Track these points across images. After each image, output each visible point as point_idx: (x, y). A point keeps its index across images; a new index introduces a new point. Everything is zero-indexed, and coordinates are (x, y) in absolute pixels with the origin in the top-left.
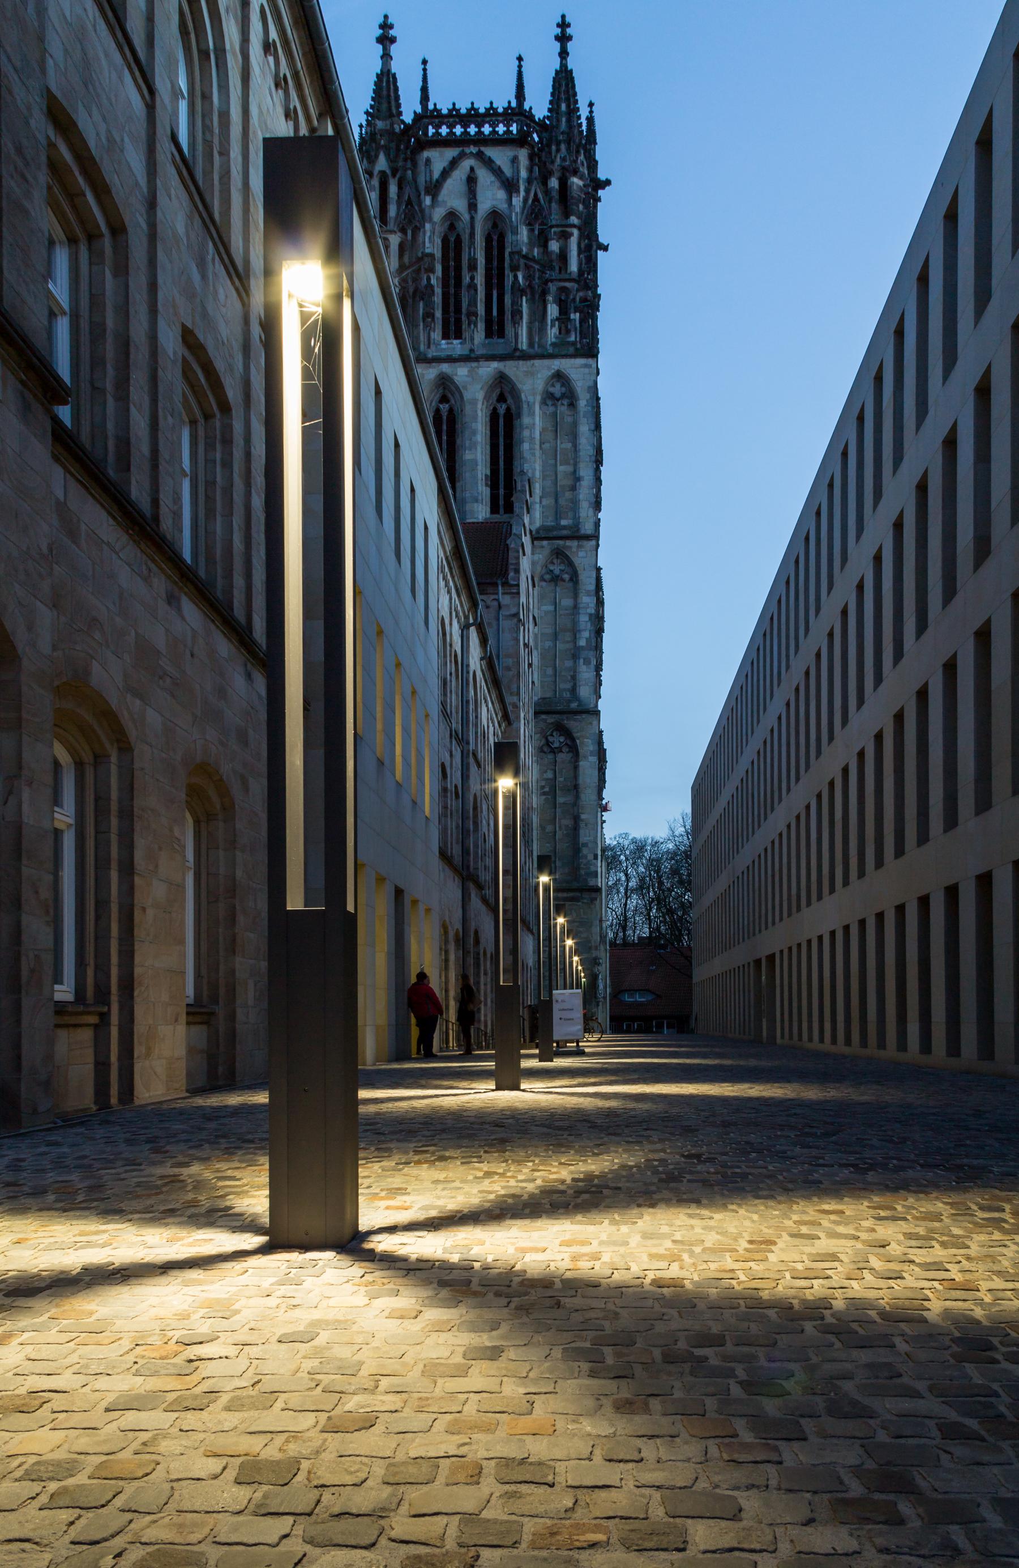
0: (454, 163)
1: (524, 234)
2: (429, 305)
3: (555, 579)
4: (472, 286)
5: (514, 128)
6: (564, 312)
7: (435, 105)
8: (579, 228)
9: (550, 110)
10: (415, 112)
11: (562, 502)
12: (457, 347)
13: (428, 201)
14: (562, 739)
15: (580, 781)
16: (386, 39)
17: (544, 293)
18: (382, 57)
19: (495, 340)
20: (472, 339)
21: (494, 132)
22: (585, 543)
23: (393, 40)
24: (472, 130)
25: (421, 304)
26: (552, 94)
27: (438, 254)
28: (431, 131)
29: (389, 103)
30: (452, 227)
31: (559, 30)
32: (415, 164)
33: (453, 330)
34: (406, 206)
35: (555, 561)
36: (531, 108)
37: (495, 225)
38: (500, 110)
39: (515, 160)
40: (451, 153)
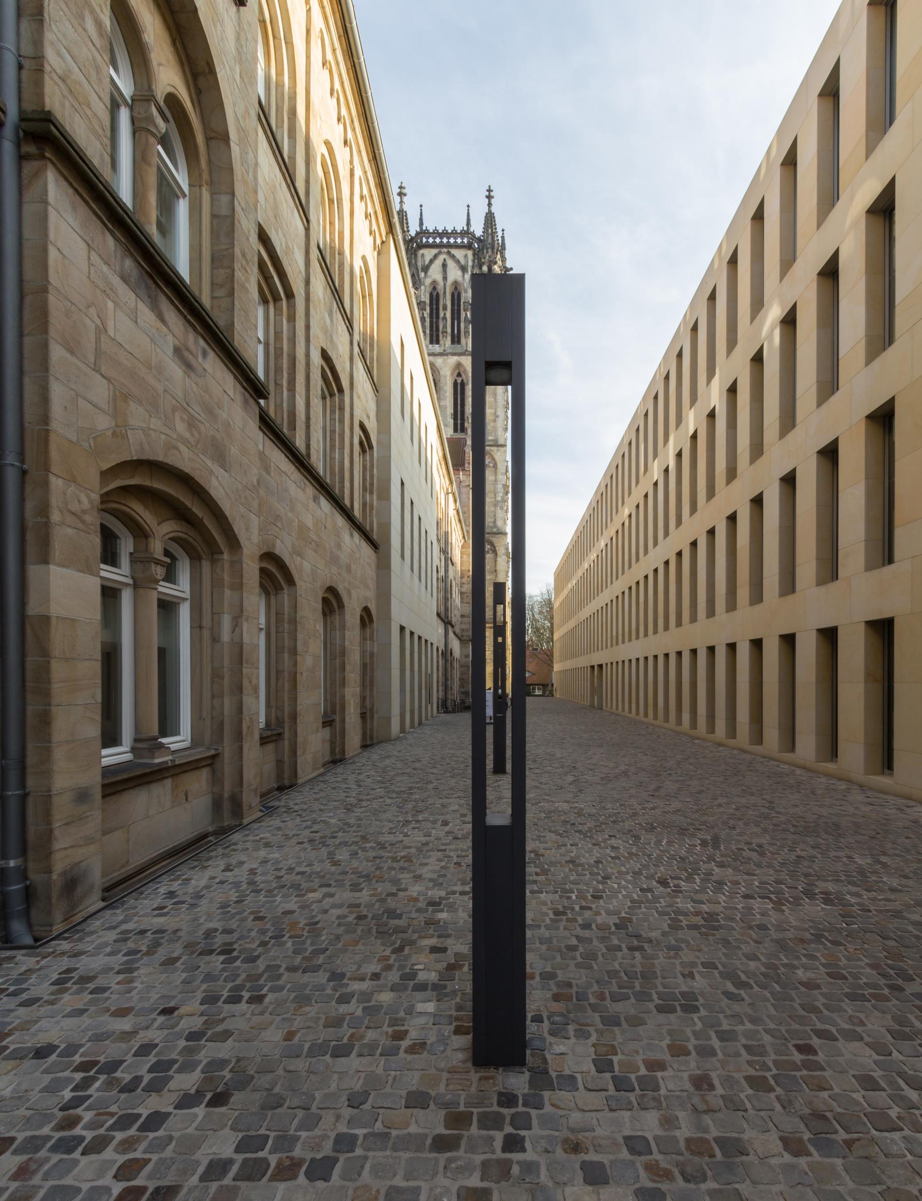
0: (436, 256)
4: (445, 318)
5: (465, 240)
13: (422, 275)
15: (498, 568)
19: (456, 345)
22: (500, 448)
27: (428, 302)
28: (424, 240)
30: (435, 288)
32: (416, 256)
37: (456, 288)
39: (466, 256)
40: (434, 251)
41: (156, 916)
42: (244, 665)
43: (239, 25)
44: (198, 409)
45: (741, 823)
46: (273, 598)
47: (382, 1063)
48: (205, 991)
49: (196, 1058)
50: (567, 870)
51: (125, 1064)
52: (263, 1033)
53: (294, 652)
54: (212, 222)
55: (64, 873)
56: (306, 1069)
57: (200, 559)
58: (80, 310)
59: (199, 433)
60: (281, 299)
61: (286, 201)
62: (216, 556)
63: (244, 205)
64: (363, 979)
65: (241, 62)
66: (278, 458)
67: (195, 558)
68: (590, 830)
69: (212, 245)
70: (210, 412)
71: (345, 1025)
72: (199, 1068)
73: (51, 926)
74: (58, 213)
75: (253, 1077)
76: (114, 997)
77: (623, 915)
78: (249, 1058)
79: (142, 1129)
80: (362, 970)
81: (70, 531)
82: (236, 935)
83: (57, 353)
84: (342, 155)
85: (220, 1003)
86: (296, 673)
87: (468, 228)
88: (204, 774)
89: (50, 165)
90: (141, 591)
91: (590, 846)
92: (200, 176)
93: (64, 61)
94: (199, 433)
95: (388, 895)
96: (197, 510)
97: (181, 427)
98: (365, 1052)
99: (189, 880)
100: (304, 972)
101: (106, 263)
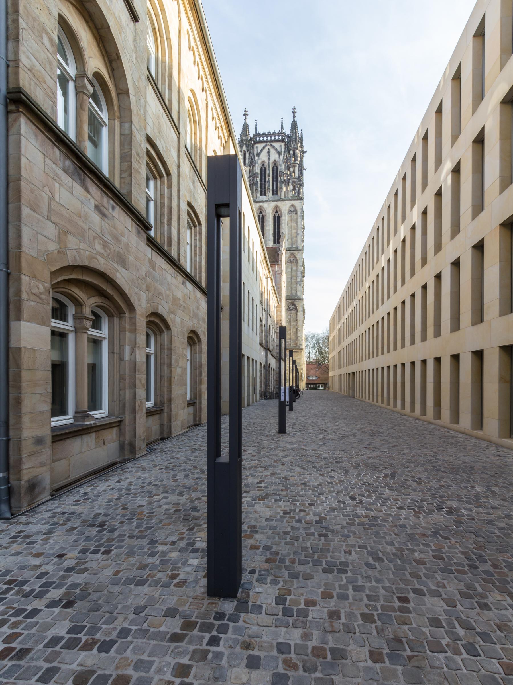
0: (264, 147)
1: (283, 166)
2: (257, 187)
3: (292, 262)
4: (269, 181)
5: (280, 137)
11: (293, 240)
12: (264, 198)
13: (256, 158)
15: (298, 318)
17: (289, 183)
19: (275, 196)
25: (255, 187)
27: (260, 173)
28: (258, 139)
30: (263, 165)
32: (253, 148)
33: (263, 193)
37: (275, 164)
39: (281, 146)
40: (263, 145)
41: (73, 505)
42: (137, 373)
43: (135, 32)
44: (109, 237)
45: (412, 465)
46: (158, 337)
47: (160, 591)
48: (83, 546)
49: (65, 581)
50: (300, 488)
51: (30, 582)
52: (104, 571)
53: (170, 366)
54: (120, 138)
55: (28, 481)
56: (119, 591)
57: (113, 316)
58: (39, 189)
59: (110, 250)
60: (164, 177)
61: (166, 123)
62: (122, 315)
63: (138, 128)
64: (166, 545)
65: (136, 52)
66: (161, 262)
67: (110, 316)
68: (322, 466)
69: (121, 150)
70: (116, 239)
71: (148, 569)
72: (65, 587)
73: (21, 508)
74: (27, 139)
75: (90, 594)
76: (37, 546)
77: (323, 515)
78: (91, 584)
79: (25, 617)
80: (167, 540)
81: (32, 303)
82: (109, 517)
83: (25, 211)
84: (201, 97)
85: (88, 553)
86: (171, 377)
87: (282, 131)
88: (115, 430)
89: (22, 115)
90: (79, 334)
91: (318, 475)
92: (114, 114)
93: (30, 60)
94: (110, 250)
95: (196, 499)
96: (110, 291)
97: (99, 247)
98: (153, 584)
99: (97, 487)
100: (137, 539)
101: (54, 163)
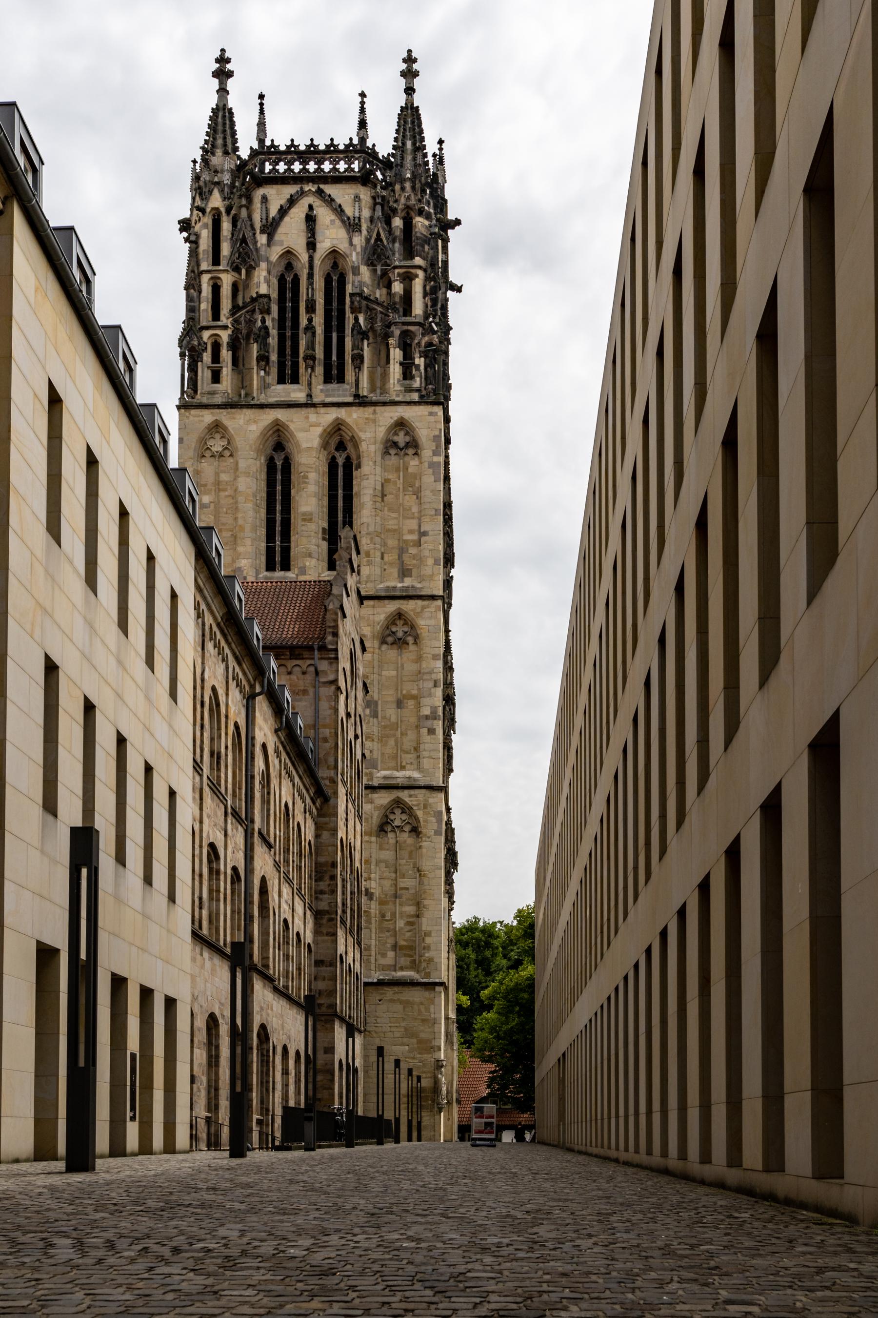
0: (292, 201)
1: (365, 272)
4: (310, 328)
5: (356, 166)
6: (408, 356)
7: (272, 141)
8: (425, 270)
9: (394, 147)
10: (251, 148)
13: (262, 239)
14: (404, 817)
16: (223, 74)
17: (387, 336)
18: (218, 91)
19: (334, 386)
20: (310, 384)
21: (335, 169)
23: (230, 74)
24: (312, 167)
26: (397, 131)
27: (274, 295)
28: (268, 167)
29: (225, 138)
30: (289, 267)
31: (404, 66)
32: (250, 200)
34: (241, 245)
35: (398, 622)
36: (374, 145)
37: (335, 265)
38: (341, 147)
39: (357, 198)
40: (290, 190)
87: (363, 140)
